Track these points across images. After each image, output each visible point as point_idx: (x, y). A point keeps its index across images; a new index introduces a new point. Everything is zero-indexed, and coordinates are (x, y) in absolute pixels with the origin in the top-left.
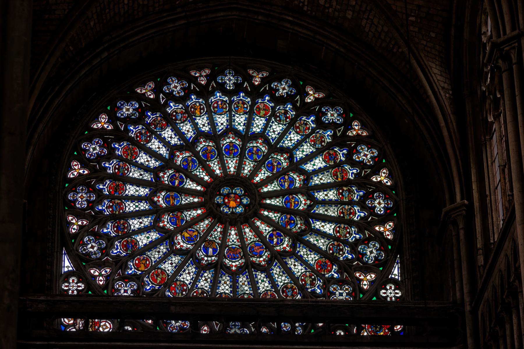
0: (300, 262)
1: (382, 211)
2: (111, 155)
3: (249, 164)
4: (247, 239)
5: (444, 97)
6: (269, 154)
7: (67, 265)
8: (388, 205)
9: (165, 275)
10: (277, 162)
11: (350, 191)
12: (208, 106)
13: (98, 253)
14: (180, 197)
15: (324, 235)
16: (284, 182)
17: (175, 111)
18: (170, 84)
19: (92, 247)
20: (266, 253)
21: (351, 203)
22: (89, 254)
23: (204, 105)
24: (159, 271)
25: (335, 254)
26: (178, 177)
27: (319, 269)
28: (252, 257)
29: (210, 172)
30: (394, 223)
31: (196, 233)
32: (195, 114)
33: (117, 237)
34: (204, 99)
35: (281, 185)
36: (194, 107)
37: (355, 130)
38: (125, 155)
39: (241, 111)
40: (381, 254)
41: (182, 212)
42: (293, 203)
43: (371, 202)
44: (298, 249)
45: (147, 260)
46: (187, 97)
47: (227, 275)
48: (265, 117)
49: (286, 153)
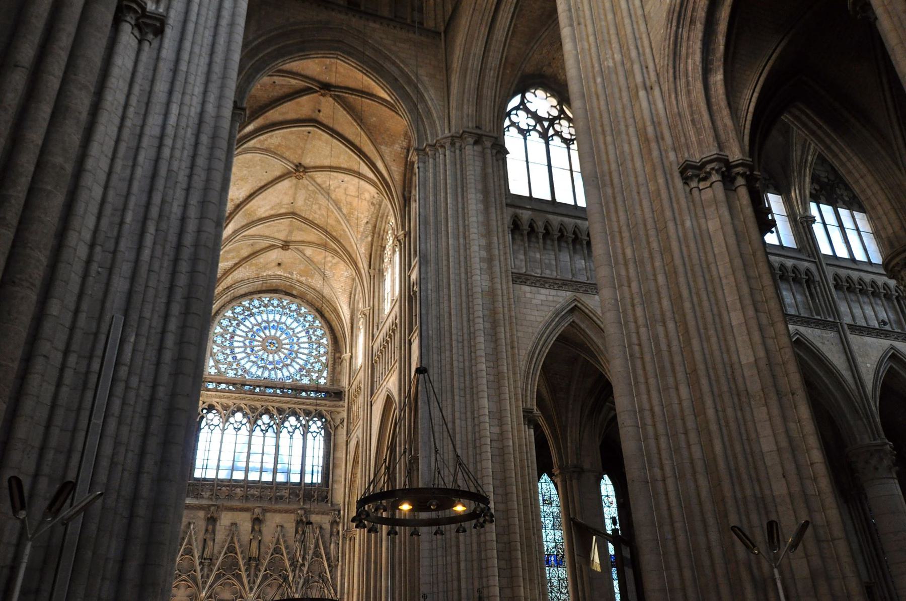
7: (211, 363)
46: (260, 307)
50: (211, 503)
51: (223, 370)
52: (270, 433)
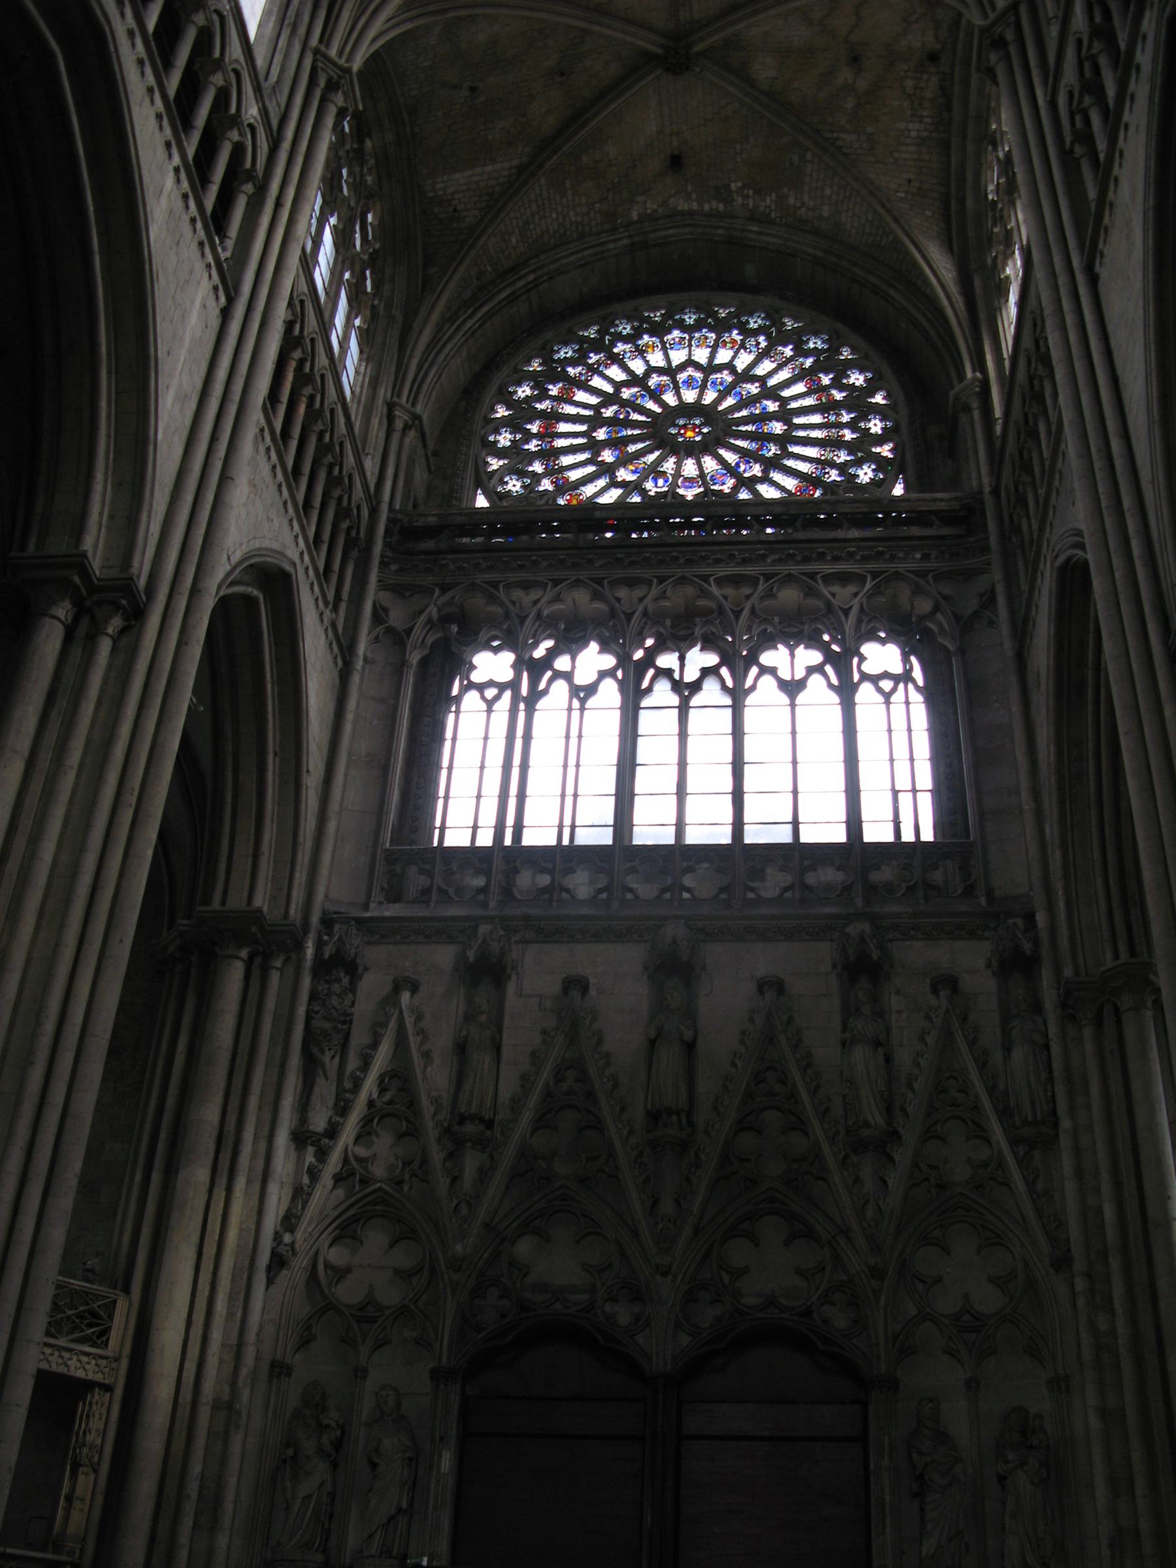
2: (543, 395)
29: (662, 404)
36: (647, 345)
41: (627, 446)
45: (581, 494)
50: (479, 912)
52: (711, 692)
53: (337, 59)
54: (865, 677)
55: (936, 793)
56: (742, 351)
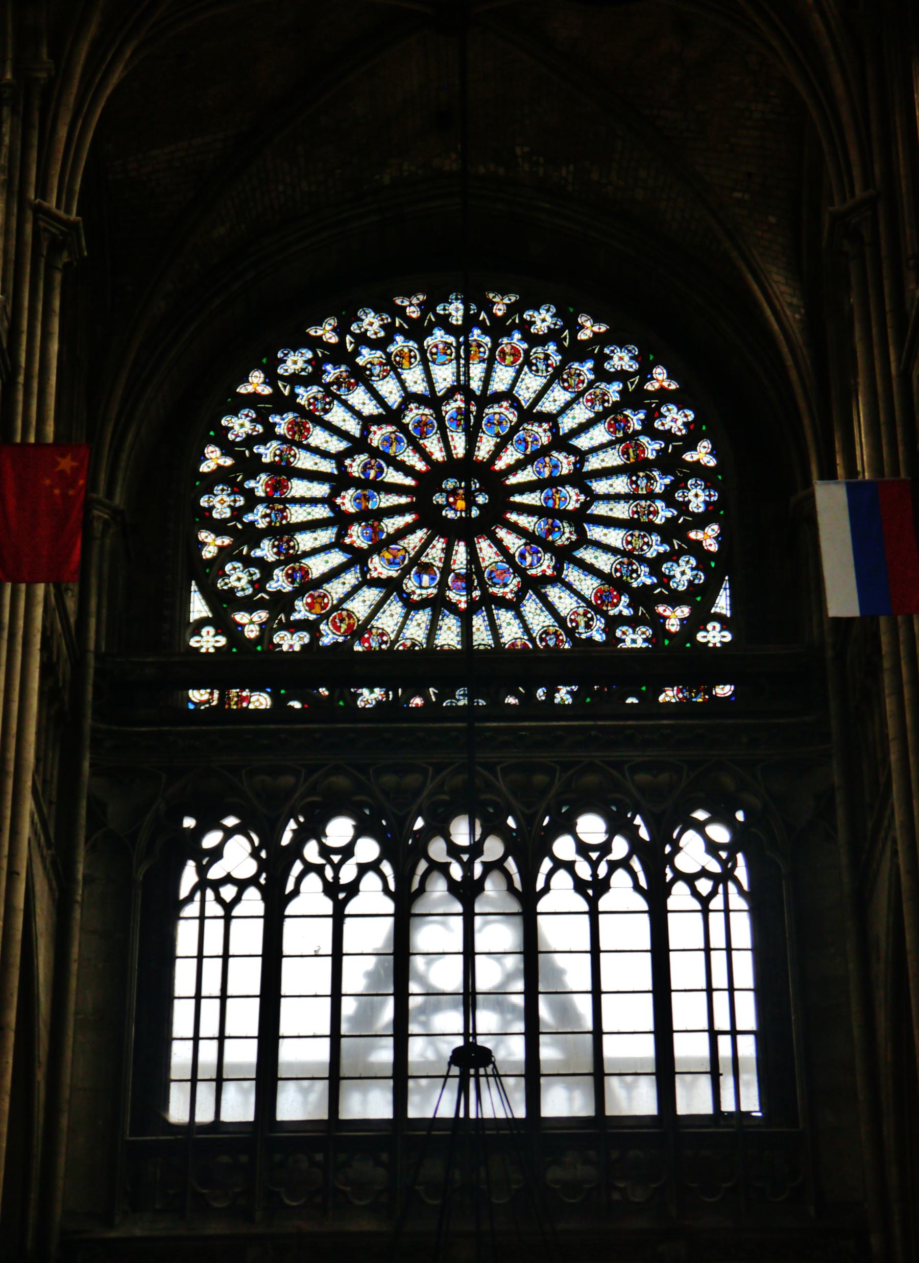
0: (568, 592)
1: (700, 507)
2: (269, 435)
3: (488, 441)
4: (483, 559)
5: (791, 320)
6: (520, 423)
7: (199, 608)
8: (710, 498)
9: (354, 619)
10: (532, 436)
11: (649, 478)
12: (422, 351)
13: (247, 588)
14: (377, 497)
15: (607, 548)
16: (545, 466)
17: (370, 363)
18: (362, 320)
19: (239, 579)
20: (514, 580)
21: (651, 496)
22: (232, 590)
23: (416, 351)
24: (344, 613)
25: (625, 578)
26: (374, 466)
27: (599, 602)
28: (491, 586)
29: (425, 456)
30: (720, 526)
31: (403, 553)
32: (402, 366)
33: (277, 564)
34: (416, 342)
35: (539, 473)
36: (400, 354)
37: (658, 380)
38: (291, 433)
39: (476, 357)
40: (699, 576)
41: (381, 520)
42: (557, 500)
43: (683, 494)
44: (565, 572)
45: (325, 596)
46: (388, 340)
47: (452, 616)
48: (513, 366)
49: (547, 422)
51: (252, 632)
53: (61, 213)
54: (679, 875)
55: (761, 1036)
56: (526, 369)
